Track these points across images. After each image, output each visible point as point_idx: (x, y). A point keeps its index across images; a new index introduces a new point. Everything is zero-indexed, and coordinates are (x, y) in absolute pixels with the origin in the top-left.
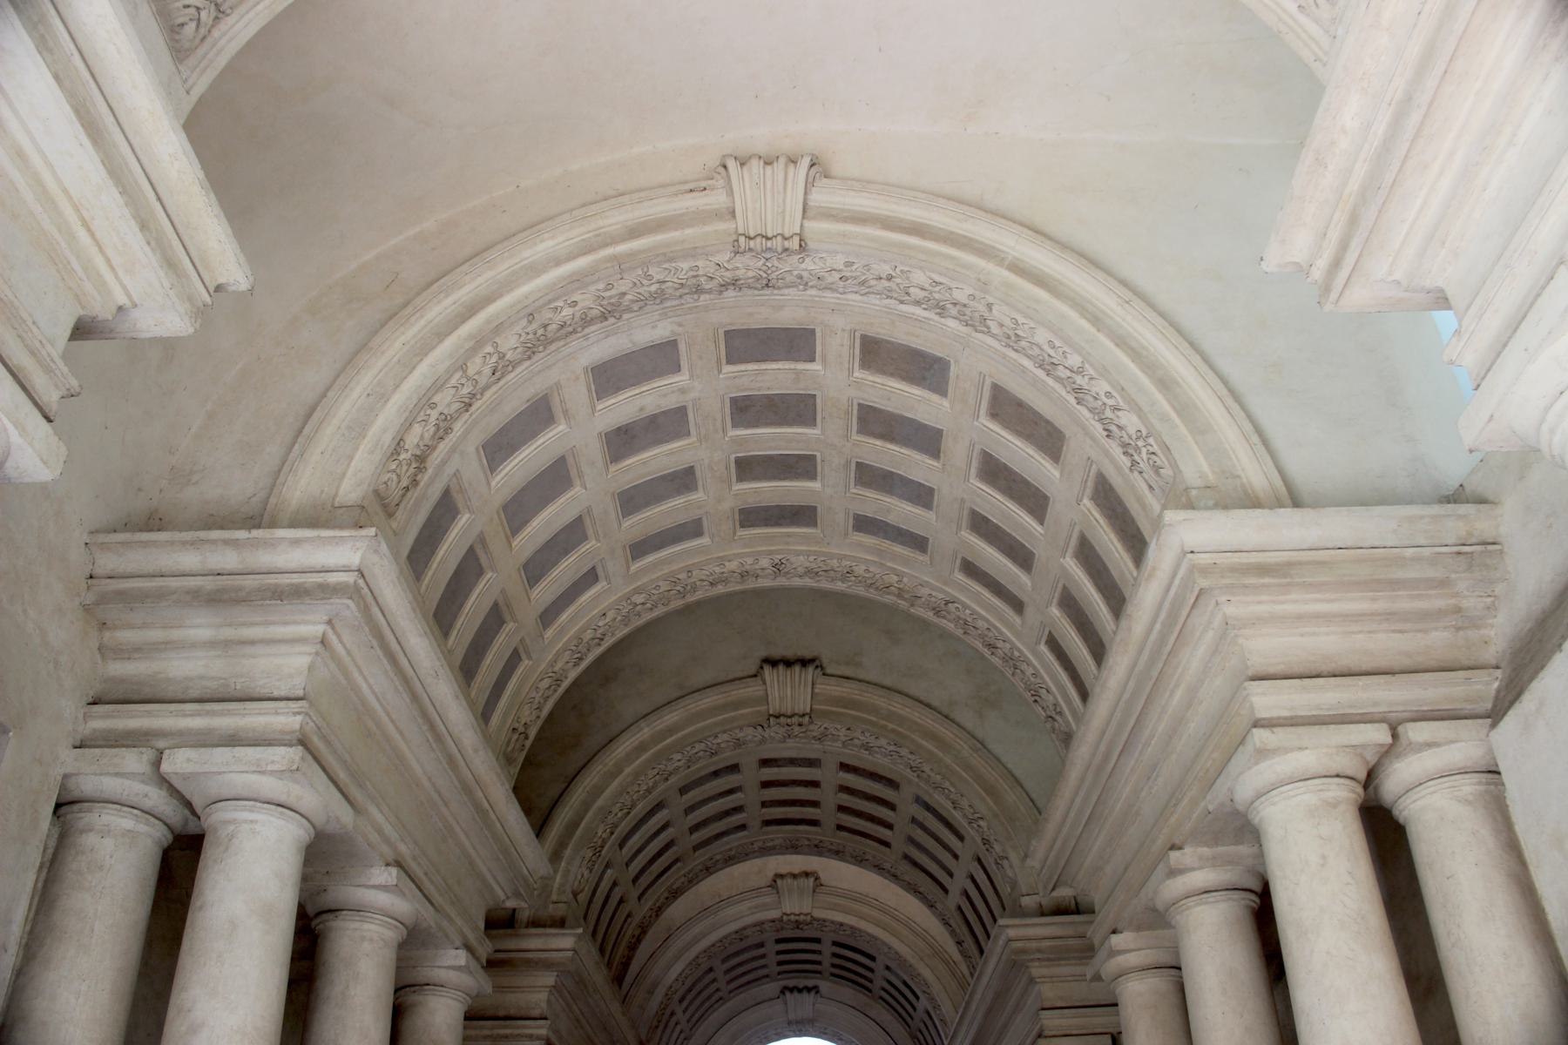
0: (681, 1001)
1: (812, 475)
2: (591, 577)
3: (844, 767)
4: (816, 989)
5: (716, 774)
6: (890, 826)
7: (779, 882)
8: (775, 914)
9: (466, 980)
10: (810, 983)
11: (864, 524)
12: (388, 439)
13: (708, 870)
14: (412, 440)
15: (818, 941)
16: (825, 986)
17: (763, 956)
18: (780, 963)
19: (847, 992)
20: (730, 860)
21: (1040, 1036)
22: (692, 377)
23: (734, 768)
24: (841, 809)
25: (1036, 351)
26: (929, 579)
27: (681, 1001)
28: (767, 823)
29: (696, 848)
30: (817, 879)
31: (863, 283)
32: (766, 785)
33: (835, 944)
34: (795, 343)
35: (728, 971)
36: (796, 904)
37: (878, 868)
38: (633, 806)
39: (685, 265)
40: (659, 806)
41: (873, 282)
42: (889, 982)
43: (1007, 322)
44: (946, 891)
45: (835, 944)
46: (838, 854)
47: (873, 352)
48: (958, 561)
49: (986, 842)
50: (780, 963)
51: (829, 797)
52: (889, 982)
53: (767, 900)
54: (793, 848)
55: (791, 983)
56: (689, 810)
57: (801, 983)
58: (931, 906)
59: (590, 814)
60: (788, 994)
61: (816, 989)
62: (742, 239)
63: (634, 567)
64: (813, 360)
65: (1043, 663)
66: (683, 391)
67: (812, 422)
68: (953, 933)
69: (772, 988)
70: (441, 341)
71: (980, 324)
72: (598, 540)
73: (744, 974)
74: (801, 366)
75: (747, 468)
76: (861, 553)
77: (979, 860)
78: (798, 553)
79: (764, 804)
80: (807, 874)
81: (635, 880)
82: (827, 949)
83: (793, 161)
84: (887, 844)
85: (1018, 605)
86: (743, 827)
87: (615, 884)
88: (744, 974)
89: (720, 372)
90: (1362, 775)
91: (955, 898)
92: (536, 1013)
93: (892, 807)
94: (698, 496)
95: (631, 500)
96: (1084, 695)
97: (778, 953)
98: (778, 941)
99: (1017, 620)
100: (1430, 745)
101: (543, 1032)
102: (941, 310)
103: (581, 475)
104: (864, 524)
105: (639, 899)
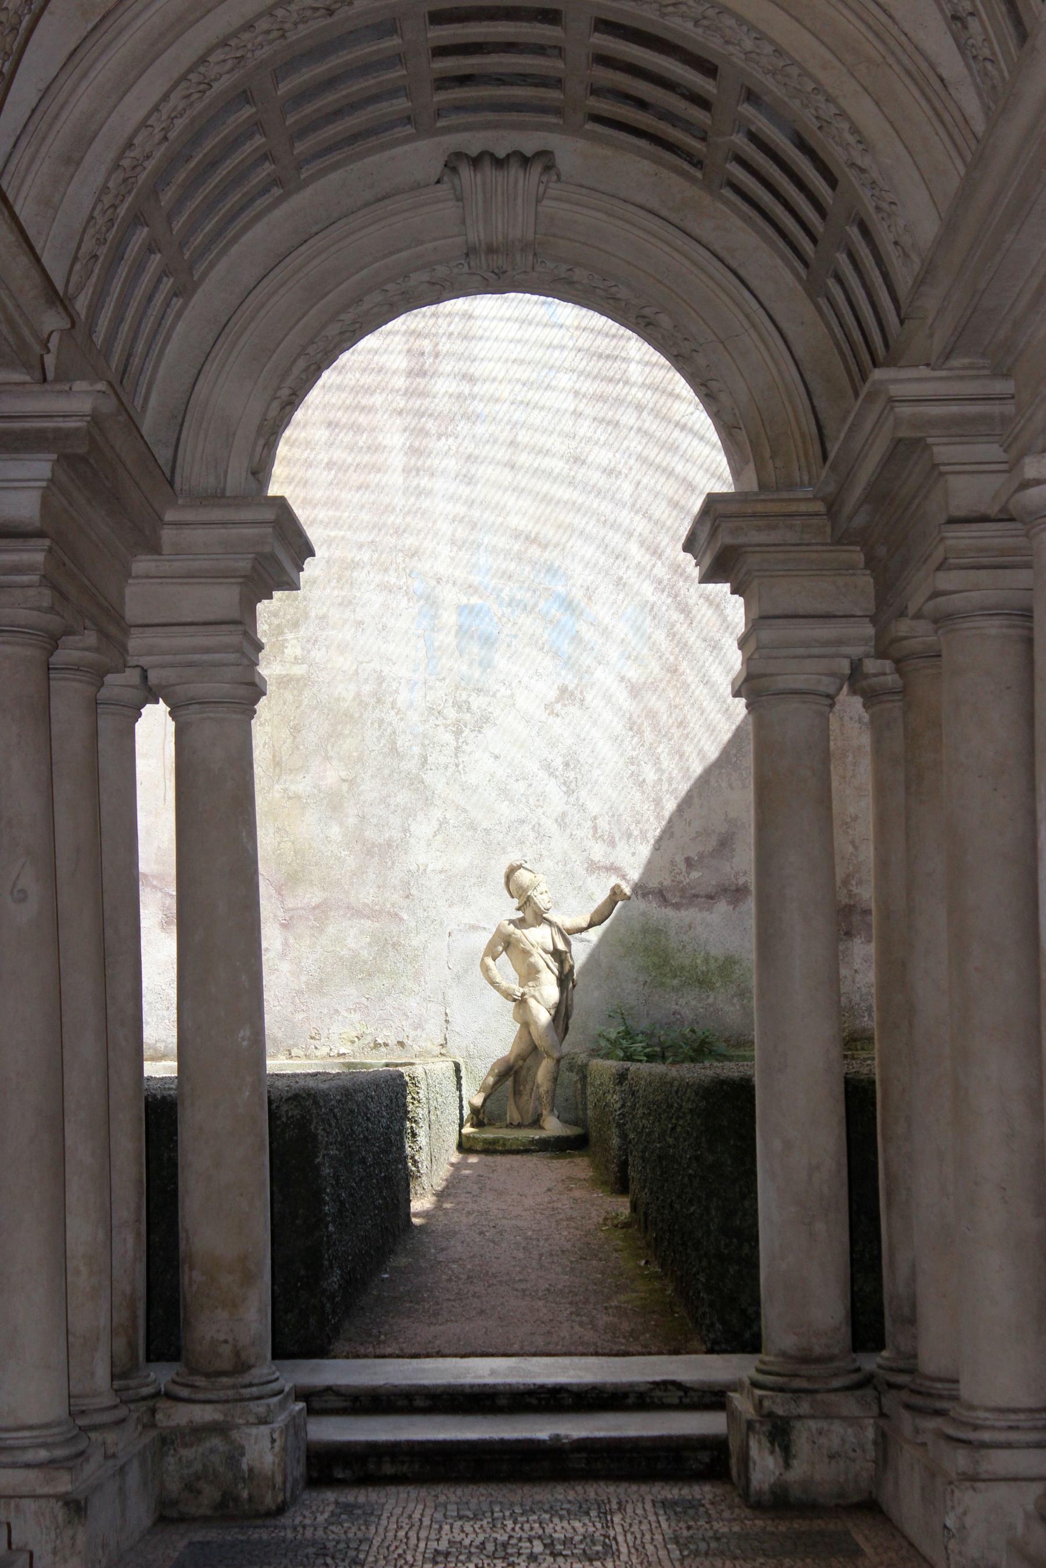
4: (545, 159)
10: (530, 143)
16: (570, 151)
18: (443, 82)
19: (634, 169)
33: (606, 26)
42: (754, 137)
45: (606, 26)
50: (443, 82)
52: (754, 137)
55: (474, 142)
57: (503, 143)
60: (466, 172)
69: (418, 157)
73: (337, 114)
82: (579, 39)
97: (441, 51)
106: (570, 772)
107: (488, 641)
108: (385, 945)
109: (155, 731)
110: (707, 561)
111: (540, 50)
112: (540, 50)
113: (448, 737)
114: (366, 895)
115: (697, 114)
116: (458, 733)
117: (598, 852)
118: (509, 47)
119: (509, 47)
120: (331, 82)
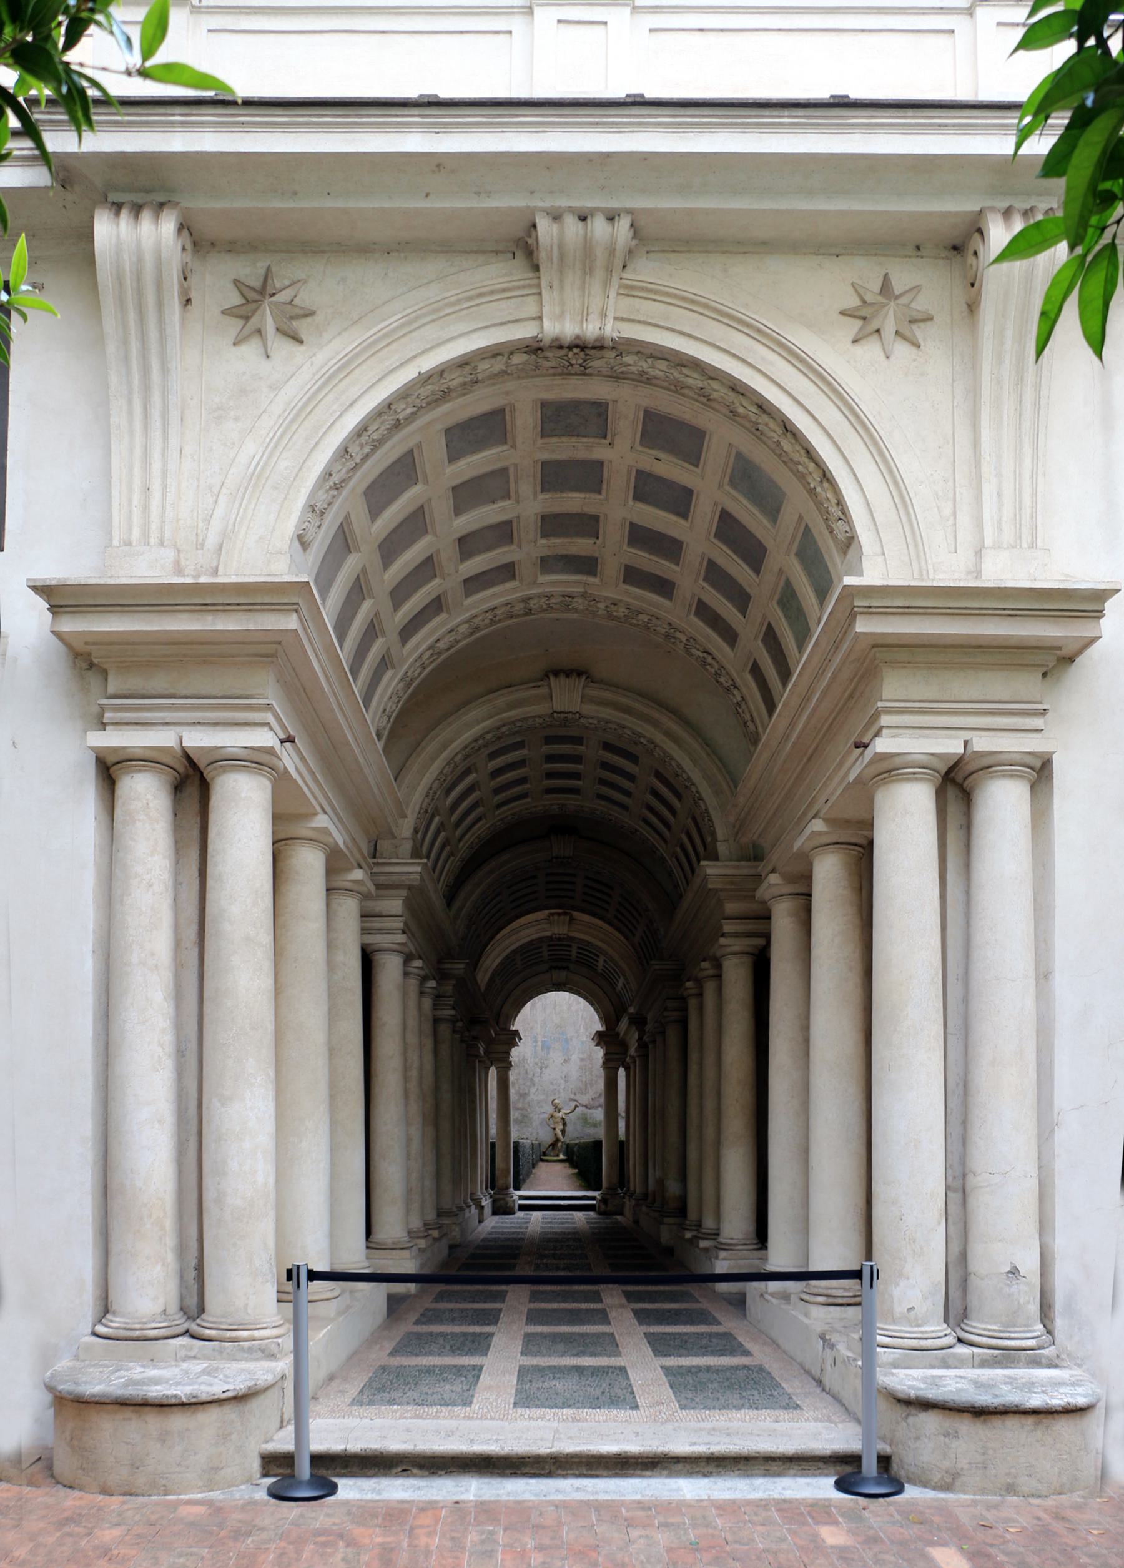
1: (579, 779)
2: (479, 819)
3: (587, 878)
6: (608, 903)
8: (548, 934)
11: (600, 796)
13: (517, 917)
21: (666, 1009)
23: (535, 877)
32: (548, 883)
36: (559, 929)
37: (602, 918)
44: (634, 935)
46: (583, 911)
47: (607, 746)
53: (545, 926)
58: (627, 939)
61: (567, 968)
64: (582, 745)
67: (580, 763)
84: (607, 910)
94: (527, 786)
95: (497, 791)
104: (600, 796)
106: (566, 1078)
107: (548, 1048)
108: (524, 1116)
109: (493, 1072)
114: (520, 1105)
117: (572, 1096)
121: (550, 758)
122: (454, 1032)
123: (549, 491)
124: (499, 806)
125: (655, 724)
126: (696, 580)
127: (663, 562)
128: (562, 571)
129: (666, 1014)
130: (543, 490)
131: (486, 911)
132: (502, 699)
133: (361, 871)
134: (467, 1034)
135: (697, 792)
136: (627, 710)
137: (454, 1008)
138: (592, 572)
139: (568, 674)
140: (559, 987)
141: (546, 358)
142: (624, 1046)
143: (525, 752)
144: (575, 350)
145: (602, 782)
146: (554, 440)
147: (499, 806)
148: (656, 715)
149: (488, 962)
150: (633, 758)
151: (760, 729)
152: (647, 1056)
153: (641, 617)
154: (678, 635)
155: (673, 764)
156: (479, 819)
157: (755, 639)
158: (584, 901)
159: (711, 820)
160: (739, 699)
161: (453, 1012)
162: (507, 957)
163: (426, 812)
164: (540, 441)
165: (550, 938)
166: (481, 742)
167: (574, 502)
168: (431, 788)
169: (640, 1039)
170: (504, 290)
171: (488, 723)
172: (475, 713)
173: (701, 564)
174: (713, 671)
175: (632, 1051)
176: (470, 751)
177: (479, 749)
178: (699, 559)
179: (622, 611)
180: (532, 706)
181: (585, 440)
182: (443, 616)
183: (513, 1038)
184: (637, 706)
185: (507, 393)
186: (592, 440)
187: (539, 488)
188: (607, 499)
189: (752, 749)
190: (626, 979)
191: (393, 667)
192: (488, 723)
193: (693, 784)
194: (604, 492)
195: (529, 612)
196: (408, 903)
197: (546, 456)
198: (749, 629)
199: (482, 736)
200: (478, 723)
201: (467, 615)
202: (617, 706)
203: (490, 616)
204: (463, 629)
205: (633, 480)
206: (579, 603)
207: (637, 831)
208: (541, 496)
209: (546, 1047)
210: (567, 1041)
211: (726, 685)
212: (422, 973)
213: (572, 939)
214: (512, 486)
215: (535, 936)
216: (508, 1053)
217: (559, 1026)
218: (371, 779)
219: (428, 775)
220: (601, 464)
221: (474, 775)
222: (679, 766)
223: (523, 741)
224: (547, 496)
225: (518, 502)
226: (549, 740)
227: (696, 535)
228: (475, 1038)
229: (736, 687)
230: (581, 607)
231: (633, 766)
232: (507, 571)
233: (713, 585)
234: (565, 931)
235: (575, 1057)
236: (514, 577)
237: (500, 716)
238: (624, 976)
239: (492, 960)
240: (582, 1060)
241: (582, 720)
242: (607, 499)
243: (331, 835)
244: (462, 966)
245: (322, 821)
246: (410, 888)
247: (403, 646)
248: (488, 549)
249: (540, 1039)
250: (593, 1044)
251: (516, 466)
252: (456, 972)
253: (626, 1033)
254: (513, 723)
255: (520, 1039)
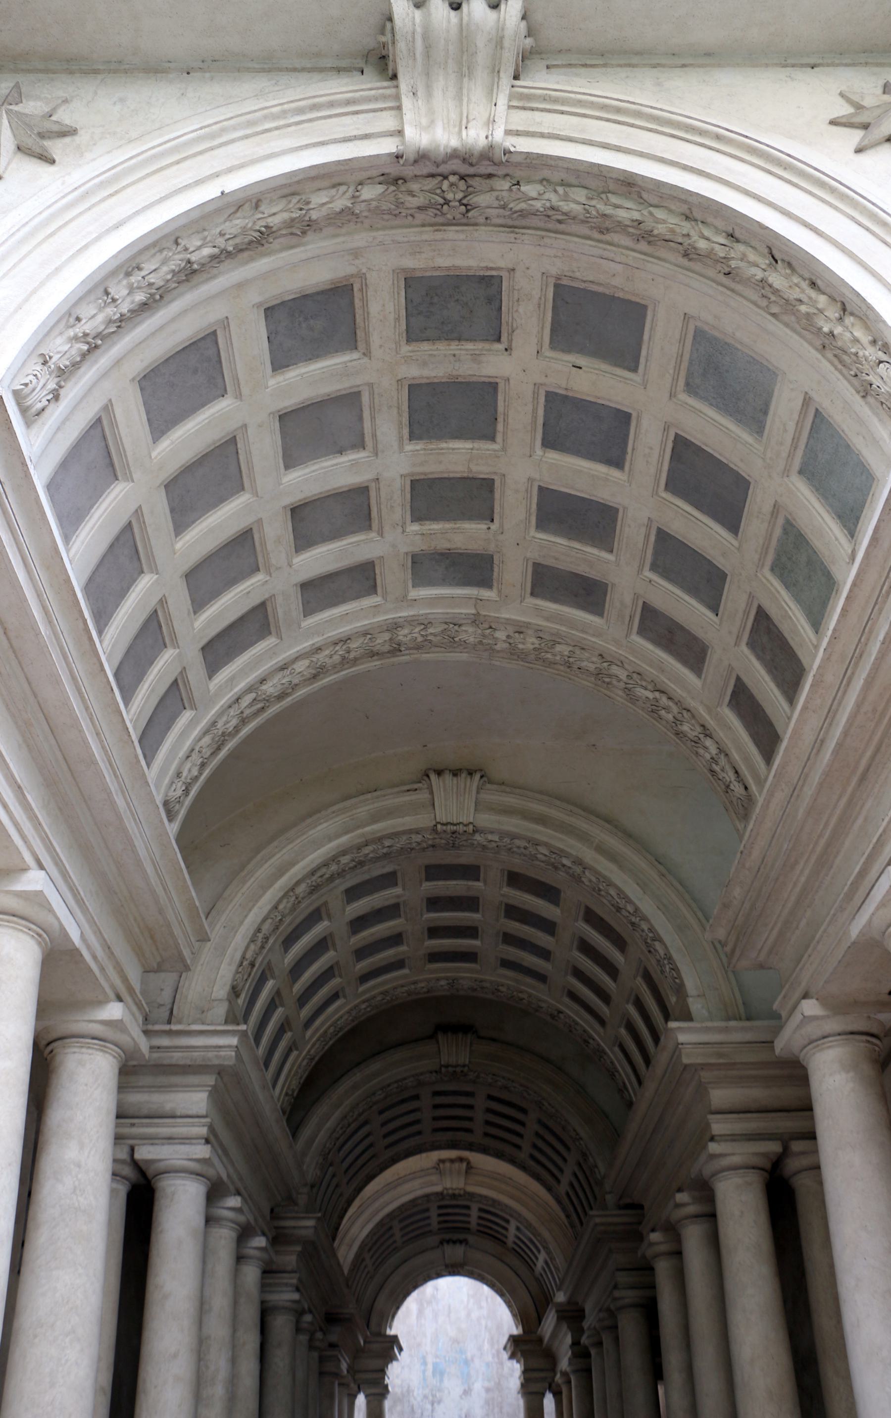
0: (369, 1250)
2: (335, 996)
3: (490, 1097)
5: (403, 1101)
7: (441, 1165)
8: (438, 1189)
9: (264, 1256)
10: (461, 1236)
11: (506, 964)
12: (238, 956)
13: (394, 1160)
14: (249, 955)
15: (468, 1207)
16: (471, 1239)
17: (428, 1218)
20: (408, 1154)
21: (616, 1287)
22: (404, 889)
23: (417, 1097)
24: (487, 1123)
25: (610, 898)
26: (546, 997)
27: (369, 1250)
28: (435, 1130)
29: (387, 1147)
30: (469, 1163)
31: (510, 849)
32: (436, 1107)
34: (471, 872)
35: (402, 1229)
36: (453, 1183)
37: (512, 1161)
38: (349, 1125)
39: (404, 838)
40: (366, 1123)
41: (515, 849)
43: (594, 879)
44: (558, 1181)
46: (485, 1150)
47: (515, 879)
48: (566, 990)
49: (584, 1155)
50: (439, 1223)
51: (480, 1116)
54: (453, 1145)
55: (447, 1236)
56: (384, 1124)
58: (549, 1189)
59: (322, 1132)
60: (445, 1245)
62: (439, 826)
63: (361, 989)
64: (478, 880)
65: (614, 1055)
66: (398, 896)
67: (476, 910)
68: (564, 1209)
70: (264, 892)
71: (578, 879)
72: (341, 976)
73: (413, 1230)
74: (470, 883)
75: (434, 932)
76: (507, 979)
77: (579, 1165)
78: (463, 978)
79: (435, 1119)
80: (461, 1159)
81: (346, 1172)
82: (474, 1213)
83: (471, 773)
85: (602, 1022)
86: (419, 1133)
87: (334, 1176)
88: (413, 1230)
89: (421, 885)
90: (768, 1166)
91: (563, 1188)
92: (289, 1268)
93: (523, 1124)
94: (403, 948)
95: (361, 953)
96: (640, 1082)
98: (440, 1207)
99: (601, 1030)
100: (803, 1153)
101: (295, 1281)
102: (556, 868)
103: (334, 945)
104: (506, 964)
105: (348, 1183)
107: (442, 1374)
109: (361, 1400)
110: (509, 1353)
111: (465, 1215)
112: (465, 1215)
113: (429, 1407)
115: (504, 1232)
116: (433, 1404)
118: (456, 1214)
119: (456, 1214)
120: (412, 1223)
121: (434, 903)
122: (298, 1330)
123: (420, 438)
124: (364, 978)
125: (583, 837)
126: (640, 570)
127: (589, 549)
128: (443, 582)
129: (617, 1294)
130: (412, 437)
131: (350, 1144)
132: (364, 808)
133: (120, 1005)
134: (319, 1335)
135: (650, 930)
136: (542, 820)
137: (298, 1289)
138: (486, 582)
139: (455, 773)
140: (454, 1269)
141: (411, 193)
142: (551, 1357)
143: (397, 891)
144: (452, 179)
145: (509, 939)
146: (425, 346)
147: (364, 978)
148: (582, 824)
149: (354, 1230)
150: (550, 893)
151: (753, 788)
152: (588, 1371)
153: (558, 648)
154: (615, 670)
155: (612, 892)
156: (335, 996)
157: (737, 644)
158: (486, 1134)
159: (675, 969)
160: (713, 750)
161: (296, 1296)
162: (381, 1224)
163: (252, 965)
164: (406, 349)
165: (440, 1195)
166: (334, 868)
167: (456, 456)
168: (259, 930)
169: (575, 1343)
170: (348, 102)
171: (344, 839)
172: (323, 828)
173: (647, 537)
174: (670, 717)
175: (564, 1364)
176: (319, 880)
177: (332, 878)
178: (643, 530)
179: (530, 642)
180: (405, 817)
181: (470, 346)
182: (270, 642)
183: (389, 1348)
184: (553, 813)
185: (356, 253)
186: (480, 345)
187: (406, 432)
188: (504, 449)
189: (740, 826)
190: (549, 1253)
191: (194, 707)
192: (344, 839)
193: (644, 918)
194: (499, 437)
195: (396, 649)
196: (216, 1096)
197: (414, 372)
198: (723, 633)
199: (334, 859)
200: (330, 840)
201: (306, 644)
202: (525, 815)
203: (340, 650)
204: (301, 666)
205: (541, 412)
206: (469, 634)
207: (560, 1012)
208: (409, 447)
209: (438, 1372)
210: (467, 1362)
211: (692, 734)
212: (242, 1219)
213: (472, 1196)
214: (367, 424)
215: (419, 1193)
216: (382, 1372)
217: (456, 1341)
218: (142, 853)
219: (255, 910)
220: (492, 387)
221: (326, 923)
222: (621, 893)
223: (393, 874)
224: (419, 446)
225: (376, 455)
226: (433, 872)
227: (638, 493)
228: (332, 1346)
229: (708, 735)
230: (472, 639)
231: (552, 907)
232: (362, 578)
233: (666, 574)
234: (461, 1185)
235: (478, 1386)
236: (373, 589)
237: (360, 831)
238: (546, 1248)
239: (358, 1227)
240: (488, 1390)
241: (477, 837)
242: (504, 449)
243: (51, 910)
244: (311, 1223)
245: (34, 880)
246: (220, 1071)
247: (210, 678)
248: (335, 535)
249: (430, 1360)
250: (505, 1355)
251: (371, 385)
252: (303, 1232)
253: (554, 1335)
254: (380, 839)
255: (401, 1349)
